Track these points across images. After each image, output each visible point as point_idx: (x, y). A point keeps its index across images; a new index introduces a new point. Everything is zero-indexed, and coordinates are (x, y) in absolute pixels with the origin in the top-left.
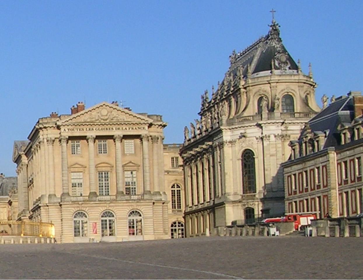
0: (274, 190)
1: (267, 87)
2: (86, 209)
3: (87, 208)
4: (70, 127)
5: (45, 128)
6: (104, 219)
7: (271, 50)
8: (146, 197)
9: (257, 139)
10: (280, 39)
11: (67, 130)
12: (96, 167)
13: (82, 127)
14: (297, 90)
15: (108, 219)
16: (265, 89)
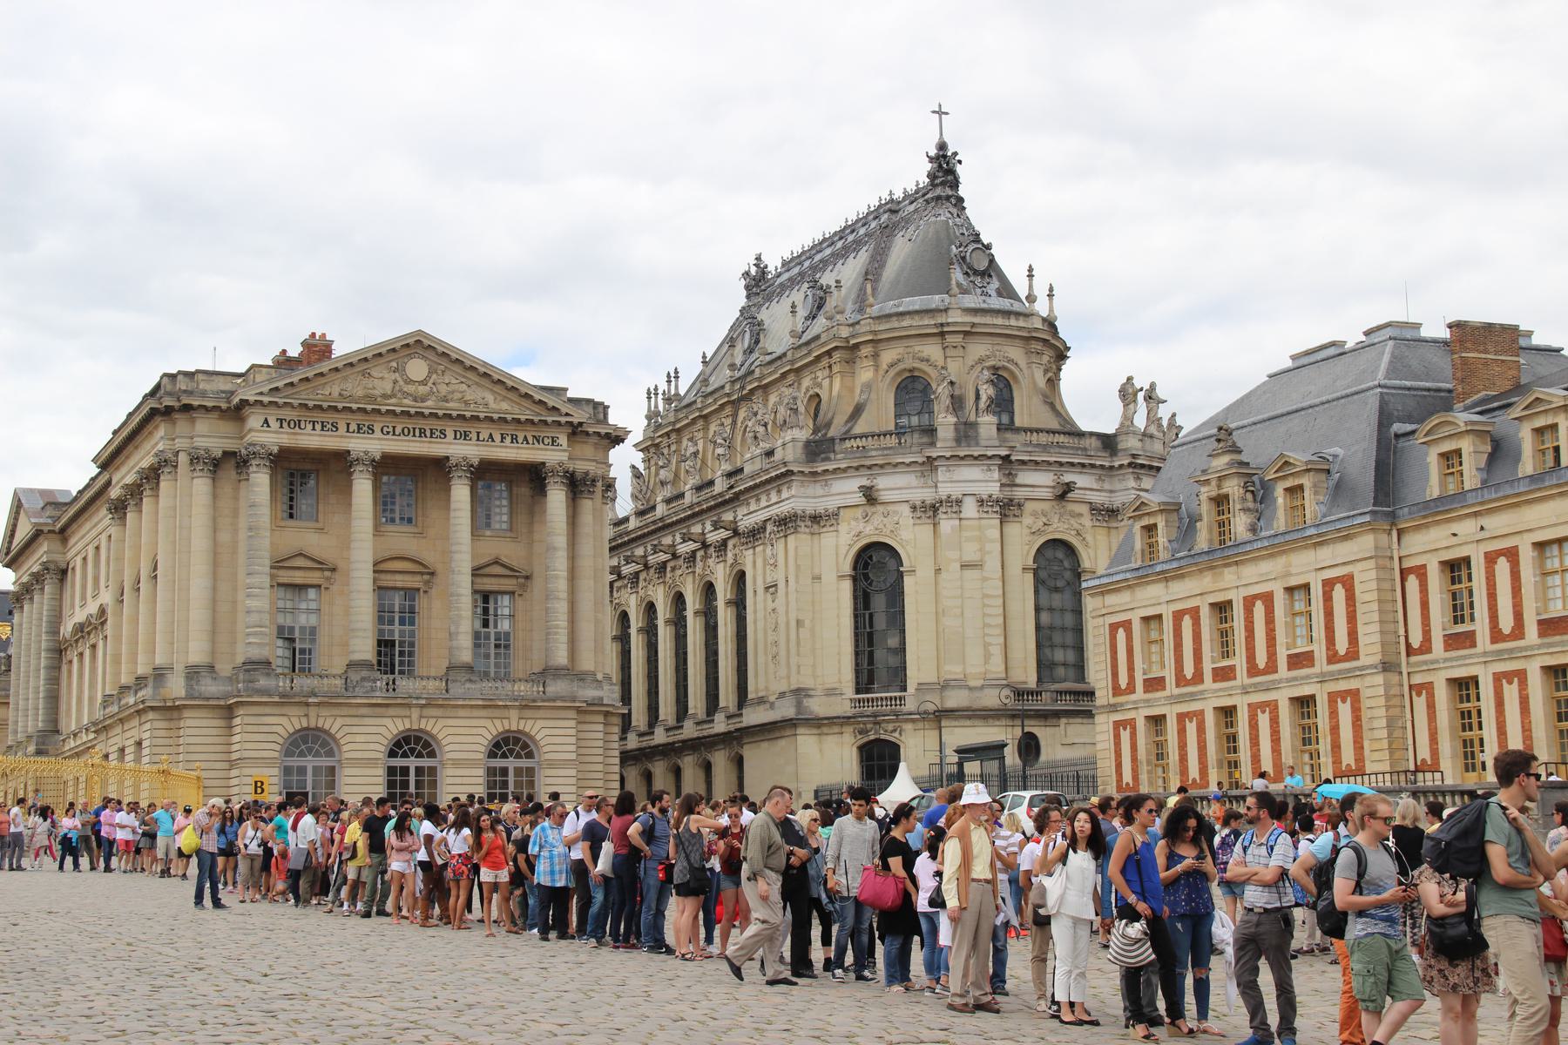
0: (972, 683)
1: (932, 350)
2: (332, 723)
3: (339, 721)
4: (288, 414)
5: (187, 408)
6: (398, 762)
7: (937, 232)
8: (556, 687)
9: (914, 508)
10: (961, 200)
11: (274, 425)
12: (378, 568)
13: (329, 417)
14: (1022, 363)
15: (412, 763)
16: (925, 355)
